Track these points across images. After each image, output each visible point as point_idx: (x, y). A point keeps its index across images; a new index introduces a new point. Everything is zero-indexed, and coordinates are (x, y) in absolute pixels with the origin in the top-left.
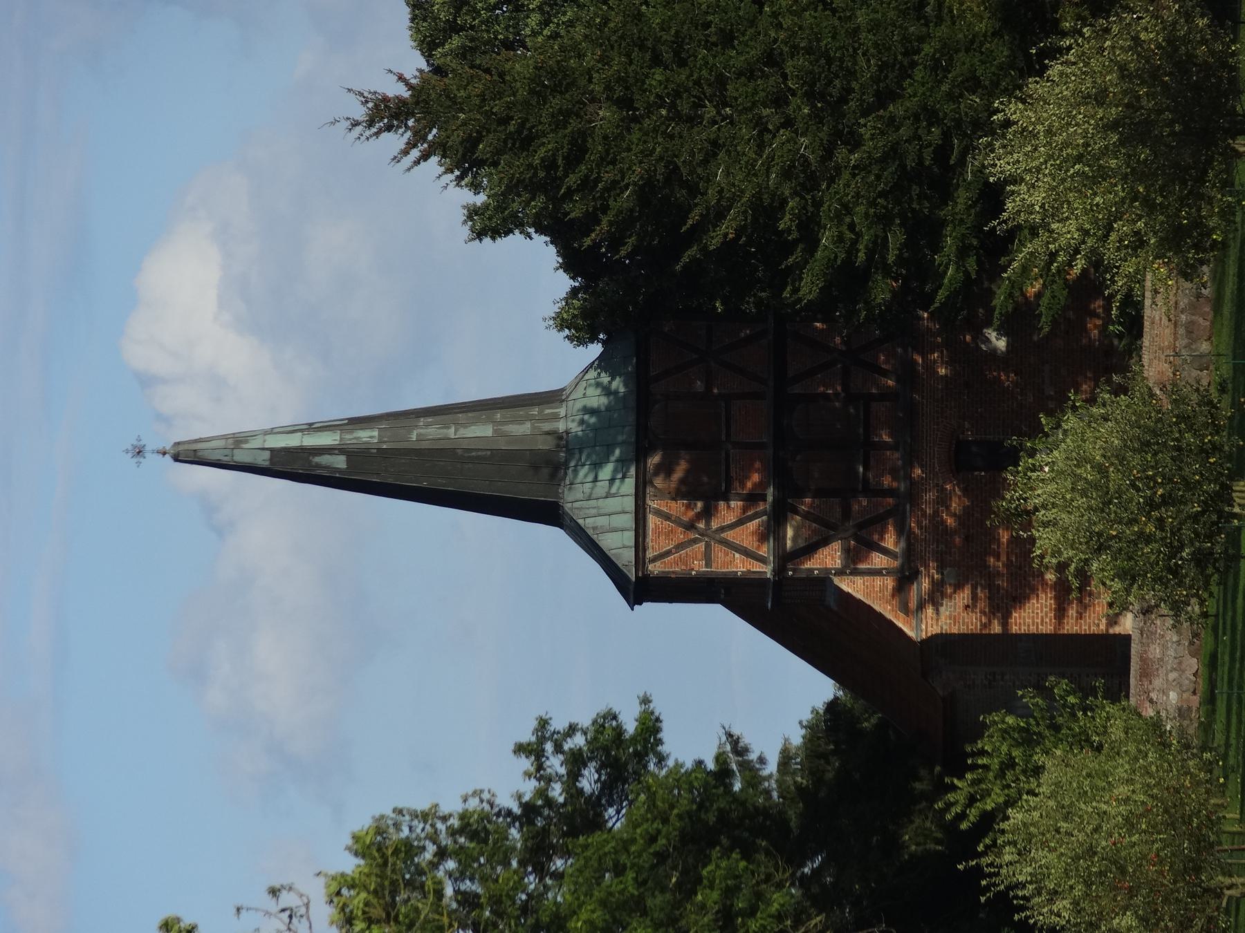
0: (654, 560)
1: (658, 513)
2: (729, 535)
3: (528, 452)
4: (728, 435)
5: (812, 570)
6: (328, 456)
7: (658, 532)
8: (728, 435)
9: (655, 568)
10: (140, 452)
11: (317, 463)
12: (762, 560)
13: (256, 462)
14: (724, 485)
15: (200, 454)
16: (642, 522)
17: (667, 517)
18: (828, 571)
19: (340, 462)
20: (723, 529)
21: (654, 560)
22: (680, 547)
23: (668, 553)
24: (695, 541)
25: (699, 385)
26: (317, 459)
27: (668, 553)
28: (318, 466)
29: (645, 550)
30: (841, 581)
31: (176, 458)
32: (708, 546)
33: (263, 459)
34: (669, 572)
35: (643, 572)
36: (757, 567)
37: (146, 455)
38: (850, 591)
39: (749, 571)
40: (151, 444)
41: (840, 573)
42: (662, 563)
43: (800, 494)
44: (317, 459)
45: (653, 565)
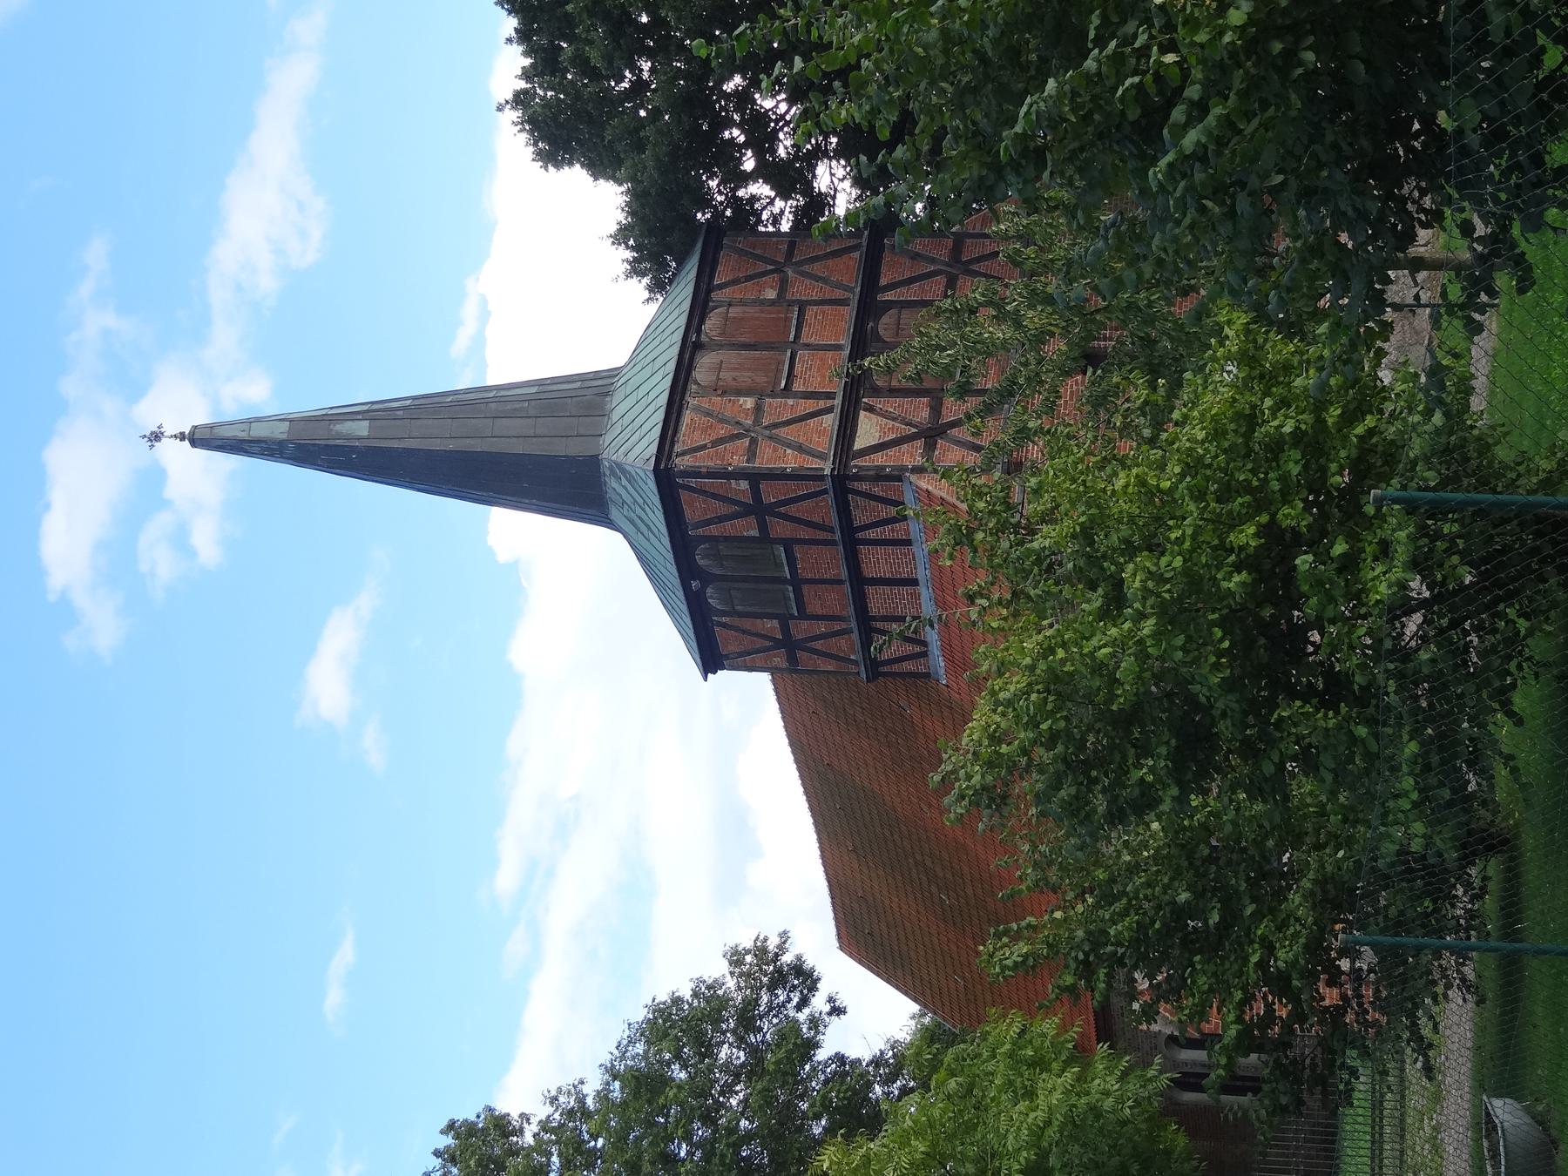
0: (684, 453)
1: (697, 409)
2: (783, 432)
3: (569, 400)
4: (797, 337)
5: (883, 468)
6: (349, 423)
7: (693, 427)
8: (797, 337)
9: (683, 463)
10: (156, 437)
11: (337, 432)
12: (823, 457)
13: (272, 435)
14: (783, 383)
15: (216, 431)
16: (674, 416)
17: (709, 414)
18: (904, 469)
19: (362, 428)
20: (776, 426)
21: (684, 453)
22: (715, 444)
23: (704, 447)
24: (738, 436)
25: (771, 294)
26: (339, 427)
27: (704, 447)
28: (339, 436)
29: (673, 443)
30: (919, 479)
31: (194, 442)
32: (754, 441)
33: (280, 432)
34: (700, 467)
35: (666, 465)
36: (815, 464)
37: (163, 440)
38: (930, 488)
39: (802, 468)
40: (170, 429)
41: (919, 470)
42: (692, 457)
43: (876, 392)
44: (339, 427)
45: (680, 459)
